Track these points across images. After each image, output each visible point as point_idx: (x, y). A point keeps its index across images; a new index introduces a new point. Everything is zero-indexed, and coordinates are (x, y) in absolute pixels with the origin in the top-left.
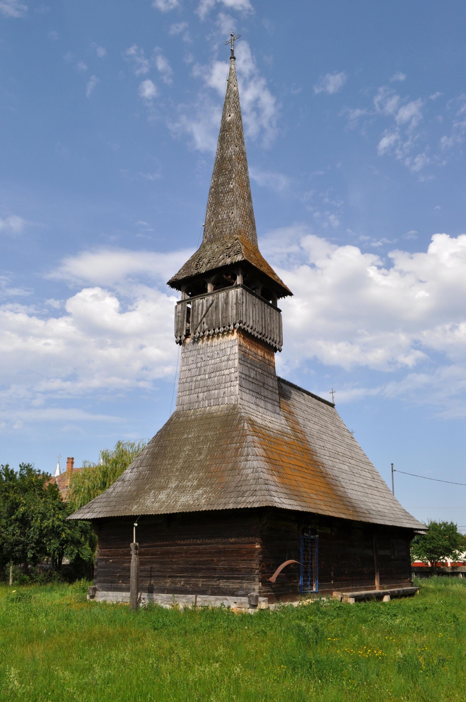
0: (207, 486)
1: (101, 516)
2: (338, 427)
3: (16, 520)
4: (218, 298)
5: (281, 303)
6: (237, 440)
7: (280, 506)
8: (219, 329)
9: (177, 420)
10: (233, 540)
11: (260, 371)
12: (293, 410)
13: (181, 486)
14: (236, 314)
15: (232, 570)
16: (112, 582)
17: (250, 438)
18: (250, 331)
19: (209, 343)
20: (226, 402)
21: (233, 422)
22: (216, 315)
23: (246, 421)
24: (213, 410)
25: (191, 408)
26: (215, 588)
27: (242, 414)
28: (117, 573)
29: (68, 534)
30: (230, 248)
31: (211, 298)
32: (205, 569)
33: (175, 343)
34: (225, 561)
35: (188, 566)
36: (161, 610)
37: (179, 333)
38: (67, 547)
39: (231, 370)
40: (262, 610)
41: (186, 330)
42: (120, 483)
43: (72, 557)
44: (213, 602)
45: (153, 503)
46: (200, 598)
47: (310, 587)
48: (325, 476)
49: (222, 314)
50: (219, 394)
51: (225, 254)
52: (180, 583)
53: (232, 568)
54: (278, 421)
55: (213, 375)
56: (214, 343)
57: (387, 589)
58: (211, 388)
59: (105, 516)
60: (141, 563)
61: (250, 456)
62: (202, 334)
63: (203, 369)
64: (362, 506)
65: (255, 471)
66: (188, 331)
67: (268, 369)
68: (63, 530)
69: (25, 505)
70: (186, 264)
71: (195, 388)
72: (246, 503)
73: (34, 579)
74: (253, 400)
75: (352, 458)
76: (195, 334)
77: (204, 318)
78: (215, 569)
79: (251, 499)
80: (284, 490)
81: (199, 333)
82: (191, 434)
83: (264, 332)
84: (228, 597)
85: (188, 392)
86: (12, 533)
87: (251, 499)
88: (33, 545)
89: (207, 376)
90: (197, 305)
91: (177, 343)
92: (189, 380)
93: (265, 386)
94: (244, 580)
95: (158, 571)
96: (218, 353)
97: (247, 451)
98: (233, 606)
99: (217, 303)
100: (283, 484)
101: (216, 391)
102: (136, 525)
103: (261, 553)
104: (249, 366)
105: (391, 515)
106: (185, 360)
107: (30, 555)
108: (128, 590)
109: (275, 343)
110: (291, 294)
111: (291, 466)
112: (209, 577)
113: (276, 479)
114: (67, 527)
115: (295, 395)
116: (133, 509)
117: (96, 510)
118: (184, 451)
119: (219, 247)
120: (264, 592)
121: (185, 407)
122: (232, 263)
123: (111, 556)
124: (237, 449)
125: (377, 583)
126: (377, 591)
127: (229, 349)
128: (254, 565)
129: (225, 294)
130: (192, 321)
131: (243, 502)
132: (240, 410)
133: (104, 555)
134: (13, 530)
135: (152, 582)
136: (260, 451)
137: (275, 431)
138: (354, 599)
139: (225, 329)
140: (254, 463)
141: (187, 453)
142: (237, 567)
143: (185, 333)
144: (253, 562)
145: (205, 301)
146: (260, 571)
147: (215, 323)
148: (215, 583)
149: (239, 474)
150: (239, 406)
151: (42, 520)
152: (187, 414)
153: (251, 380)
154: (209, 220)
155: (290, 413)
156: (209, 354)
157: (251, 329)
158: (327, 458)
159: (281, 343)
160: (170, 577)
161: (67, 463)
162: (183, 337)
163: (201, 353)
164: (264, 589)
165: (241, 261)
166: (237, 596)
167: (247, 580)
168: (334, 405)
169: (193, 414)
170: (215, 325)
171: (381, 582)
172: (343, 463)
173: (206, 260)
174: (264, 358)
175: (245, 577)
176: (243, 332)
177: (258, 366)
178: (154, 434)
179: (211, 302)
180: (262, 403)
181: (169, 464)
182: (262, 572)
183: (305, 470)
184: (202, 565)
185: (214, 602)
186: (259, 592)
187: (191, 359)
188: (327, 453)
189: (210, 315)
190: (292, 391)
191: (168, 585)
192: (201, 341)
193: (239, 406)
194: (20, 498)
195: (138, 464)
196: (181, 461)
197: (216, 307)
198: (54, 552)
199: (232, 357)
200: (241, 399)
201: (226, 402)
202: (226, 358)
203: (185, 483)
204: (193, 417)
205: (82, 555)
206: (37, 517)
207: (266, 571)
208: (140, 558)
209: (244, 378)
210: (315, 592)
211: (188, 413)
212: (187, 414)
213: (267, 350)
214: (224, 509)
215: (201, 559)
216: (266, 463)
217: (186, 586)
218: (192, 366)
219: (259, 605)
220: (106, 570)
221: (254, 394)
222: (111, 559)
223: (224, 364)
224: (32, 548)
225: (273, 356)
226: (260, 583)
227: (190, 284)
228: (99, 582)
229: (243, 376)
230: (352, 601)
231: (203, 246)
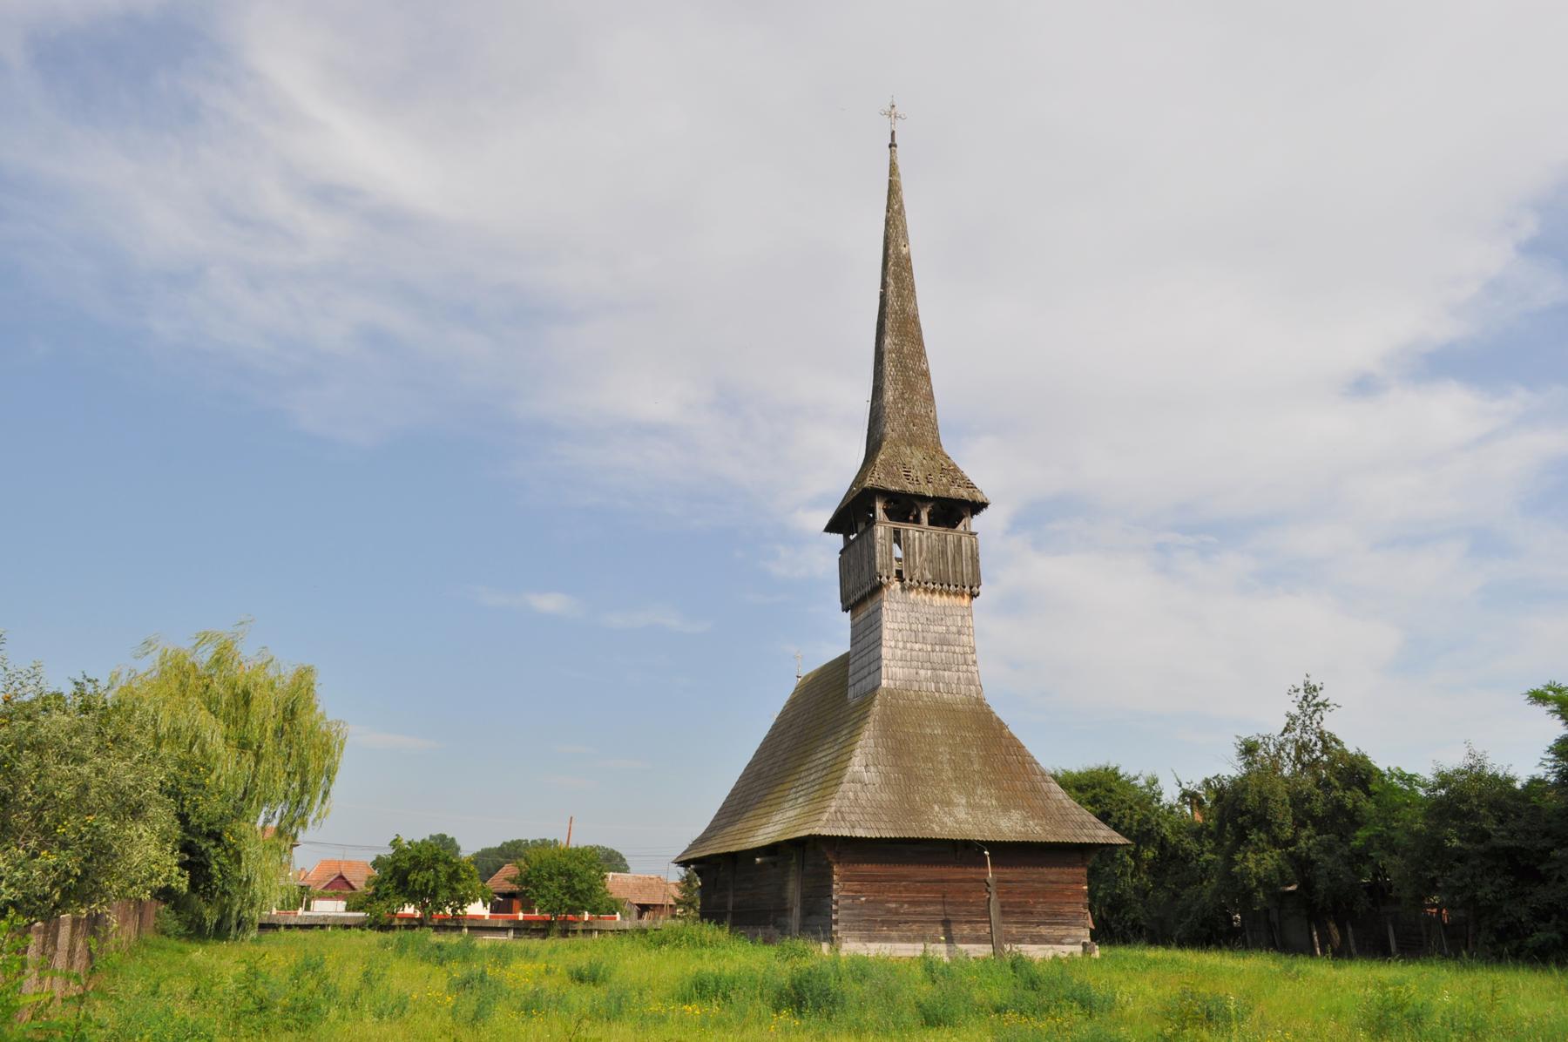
92: (901, 645)
202: (954, 629)
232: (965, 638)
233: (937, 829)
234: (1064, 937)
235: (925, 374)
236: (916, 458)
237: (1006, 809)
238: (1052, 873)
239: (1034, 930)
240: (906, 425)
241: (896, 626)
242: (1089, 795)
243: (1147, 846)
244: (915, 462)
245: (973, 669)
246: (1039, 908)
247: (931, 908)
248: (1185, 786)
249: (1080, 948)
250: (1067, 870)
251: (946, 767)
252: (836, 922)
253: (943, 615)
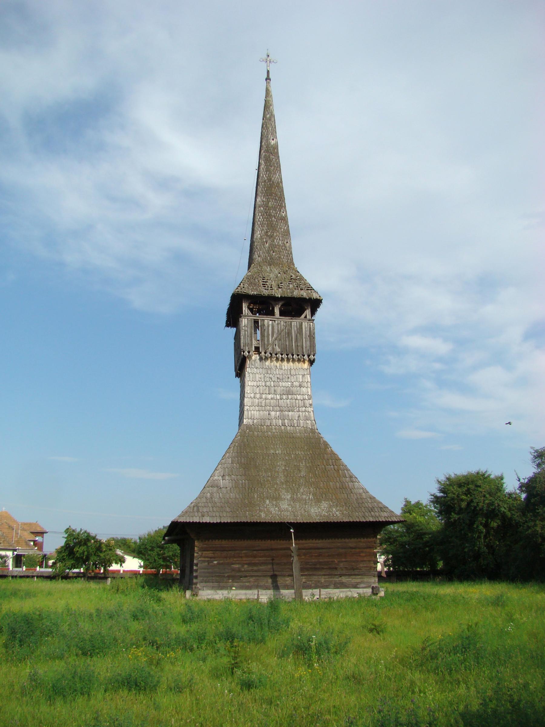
8: (293, 355)
14: (310, 346)
20: (302, 425)
28: (223, 573)
32: (326, 569)
34: (345, 561)
35: (308, 566)
39: (304, 396)
40: (380, 597)
46: (324, 591)
76: (265, 353)
81: (270, 353)
84: (351, 590)
92: (258, 396)
96: (288, 378)
101: (290, 413)
121: (255, 421)
127: (301, 376)
133: (205, 557)
148: (337, 580)
163: (269, 372)
201: (302, 425)
202: (297, 384)
232: (304, 390)
233: (263, 515)
234: (358, 583)
235: (285, 219)
236: (273, 274)
237: (318, 501)
238: (352, 542)
239: (337, 579)
240: (268, 252)
241: (255, 384)
242: (464, 489)
243: (492, 519)
244: (272, 275)
245: (310, 409)
246: (342, 565)
247: (263, 567)
248: (522, 481)
249: (369, 590)
250: (362, 540)
251: (281, 475)
252: (196, 577)
253: (290, 374)
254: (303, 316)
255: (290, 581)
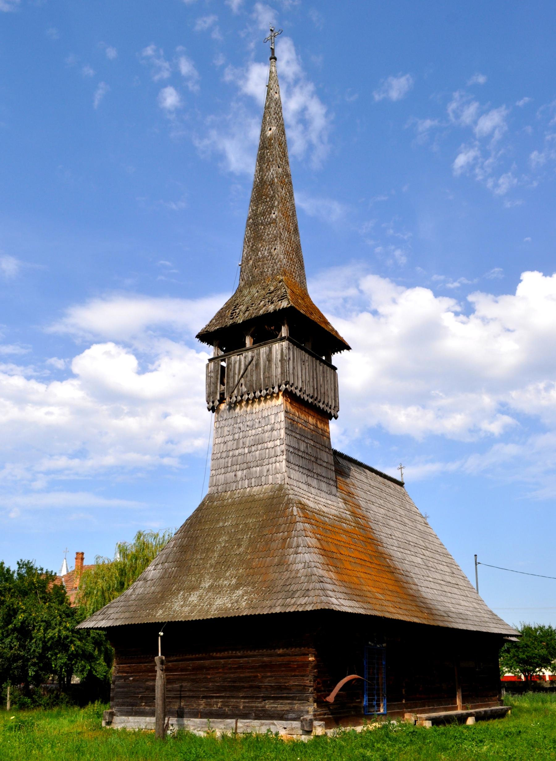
0: (248, 585)
1: (118, 623)
2: (409, 511)
3: (14, 630)
4: (259, 354)
5: (337, 359)
6: (284, 528)
7: (338, 608)
8: (261, 392)
9: (210, 504)
10: (280, 651)
11: (312, 443)
12: (352, 490)
13: (216, 585)
14: (282, 373)
15: (280, 688)
16: (132, 705)
17: (300, 526)
18: (298, 394)
19: (249, 409)
21: (280, 506)
22: (257, 374)
23: (295, 505)
24: (254, 492)
25: (227, 490)
26: (259, 711)
27: (291, 496)
29: (78, 646)
30: (273, 292)
31: (250, 354)
32: (247, 688)
33: (207, 410)
34: (271, 677)
35: (226, 684)
36: (193, 737)
37: (211, 398)
38: (76, 662)
39: (276, 442)
40: (317, 736)
41: (220, 394)
42: (141, 582)
43: (83, 674)
44: (257, 728)
45: (182, 606)
46: (242, 723)
47: (376, 708)
48: (394, 571)
49: (264, 373)
50: (261, 471)
51: (267, 300)
52: (217, 705)
53: (281, 686)
54: (335, 504)
55: (253, 448)
56: (254, 410)
57: (471, 709)
58: (252, 465)
59: (123, 624)
60: (168, 681)
61: (300, 548)
62: (239, 398)
63: (241, 441)
64: (439, 607)
65: (307, 565)
66: (223, 394)
67: (321, 439)
68: (72, 642)
69: (24, 612)
70: (219, 312)
71: (232, 465)
72: (296, 606)
73: (36, 702)
74: (304, 478)
75: (426, 548)
76: (231, 398)
77: (242, 379)
78: (259, 687)
79: (303, 601)
80: (343, 589)
81: (236, 397)
82: (228, 522)
83: (316, 395)
84: (275, 722)
85: (223, 471)
86: (9, 645)
87: (303, 601)
88: (35, 660)
89: (246, 450)
90: (233, 363)
91: (209, 410)
92: (224, 455)
93: (319, 461)
94: (295, 700)
95: (190, 691)
96: (259, 422)
97: (297, 542)
98: (282, 733)
99: (258, 360)
100: (342, 581)
101: (258, 468)
102: (161, 634)
103: (315, 667)
104: (298, 436)
105: (475, 618)
106: (219, 430)
107: (31, 673)
108: (152, 714)
109: (330, 408)
110: (348, 348)
111: (351, 559)
112: (252, 697)
113: (332, 575)
114: (77, 638)
115: (355, 472)
116: (158, 614)
117: (111, 617)
118: (220, 543)
119: (260, 291)
120: (319, 715)
121: (220, 488)
122: (275, 311)
123: (131, 673)
124: (285, 540)
125: (459, 702)
126: (459, 711)
127: (273, 416)
128: (308, 682)
129: (267, 348)
130: (228, 382)
131: (293, 605)
132: (287, 491)
133: (122, 672)
134: (10, 642)
135: (182, 704)
136: (312, 541)
137: (331, 517)
138: (430, 722)
139: (268, 391)
140: (306, 557)
141: (223, 545)
142: (287, 684)
143: (218, 398)
144: (306, 678)
145: (242, 358)
146: (315, 689)
147: (256, 384)
148: (259, 705)
149: (287, 570)
150: (286, 486)
151: (45, 630)
152: (223, 497)
153: (300, 454)
154: (247, 258)
155: (349, 494)
156: (248, 423)
157: (300, 391)
158: (396, 549)
159: (336, 408)
160: (204, 697)
161: (76, 559)
162: (217, 403)
163: (239, 421)
164: (320, 711)
165: (286, 308)
166: (287, 719)
167: (299, 700)
168: (403, 484)
169: (231, 497)
170: (256, 387)
171: (465, 700)
172: (416, 555)
173: (243, 308)
174: (317, 427)
175: (296, 697)
176: (290, 395)
177: (309, 437)
178: (183, 522)
179: (250, 359)
180: (314, 483)
181: (201, 559)
182: (317, 690)
183: (368, 564)
184: (243, 682)
185: (259, 727)
186: (314, 715)
187: (226, 429)
188: (396, 543)
189: (249, 375)
190: (352, 468)
191: (201, 707)
192: (239, 408)
193: (286, 486)
194: (18, 603)
195: (163, 559)
196: (216, 555)
197: (256, 364)
198: (61, 668)
199: (277, 426)
200: (289, 477)
202: (269, 427)
203: (221, 582)
204: (230, 500)
205: (96, 672)
206: (40, 626)
207: (322, 689)
208: (166, 675)
209: (293, 452)
210: (383, 714)
211: (224, 495)
212: (223, 497)
213: (319, 417)
214: (270, 613)
215: (242, 675)
216: (321, 556)
217: (224, 708)
218: (227, 438)
219: (314, 731)
220: (126, 690)
221: (305, 471)
222: (132, 676)
223: (267, 434)
224: (34, 664)
225: (327, 424)
226: (315, 704)
227: (224, 337)
228: (117, 705)
229: (291, 450)
230: (428, 724)
231: (240, 290)
254: (278, 338)
255: (204, 705)
